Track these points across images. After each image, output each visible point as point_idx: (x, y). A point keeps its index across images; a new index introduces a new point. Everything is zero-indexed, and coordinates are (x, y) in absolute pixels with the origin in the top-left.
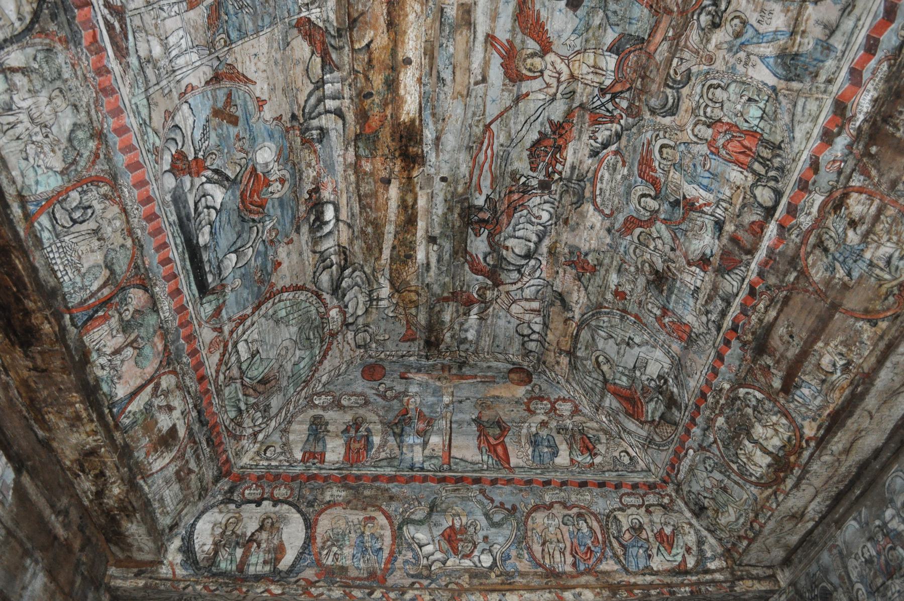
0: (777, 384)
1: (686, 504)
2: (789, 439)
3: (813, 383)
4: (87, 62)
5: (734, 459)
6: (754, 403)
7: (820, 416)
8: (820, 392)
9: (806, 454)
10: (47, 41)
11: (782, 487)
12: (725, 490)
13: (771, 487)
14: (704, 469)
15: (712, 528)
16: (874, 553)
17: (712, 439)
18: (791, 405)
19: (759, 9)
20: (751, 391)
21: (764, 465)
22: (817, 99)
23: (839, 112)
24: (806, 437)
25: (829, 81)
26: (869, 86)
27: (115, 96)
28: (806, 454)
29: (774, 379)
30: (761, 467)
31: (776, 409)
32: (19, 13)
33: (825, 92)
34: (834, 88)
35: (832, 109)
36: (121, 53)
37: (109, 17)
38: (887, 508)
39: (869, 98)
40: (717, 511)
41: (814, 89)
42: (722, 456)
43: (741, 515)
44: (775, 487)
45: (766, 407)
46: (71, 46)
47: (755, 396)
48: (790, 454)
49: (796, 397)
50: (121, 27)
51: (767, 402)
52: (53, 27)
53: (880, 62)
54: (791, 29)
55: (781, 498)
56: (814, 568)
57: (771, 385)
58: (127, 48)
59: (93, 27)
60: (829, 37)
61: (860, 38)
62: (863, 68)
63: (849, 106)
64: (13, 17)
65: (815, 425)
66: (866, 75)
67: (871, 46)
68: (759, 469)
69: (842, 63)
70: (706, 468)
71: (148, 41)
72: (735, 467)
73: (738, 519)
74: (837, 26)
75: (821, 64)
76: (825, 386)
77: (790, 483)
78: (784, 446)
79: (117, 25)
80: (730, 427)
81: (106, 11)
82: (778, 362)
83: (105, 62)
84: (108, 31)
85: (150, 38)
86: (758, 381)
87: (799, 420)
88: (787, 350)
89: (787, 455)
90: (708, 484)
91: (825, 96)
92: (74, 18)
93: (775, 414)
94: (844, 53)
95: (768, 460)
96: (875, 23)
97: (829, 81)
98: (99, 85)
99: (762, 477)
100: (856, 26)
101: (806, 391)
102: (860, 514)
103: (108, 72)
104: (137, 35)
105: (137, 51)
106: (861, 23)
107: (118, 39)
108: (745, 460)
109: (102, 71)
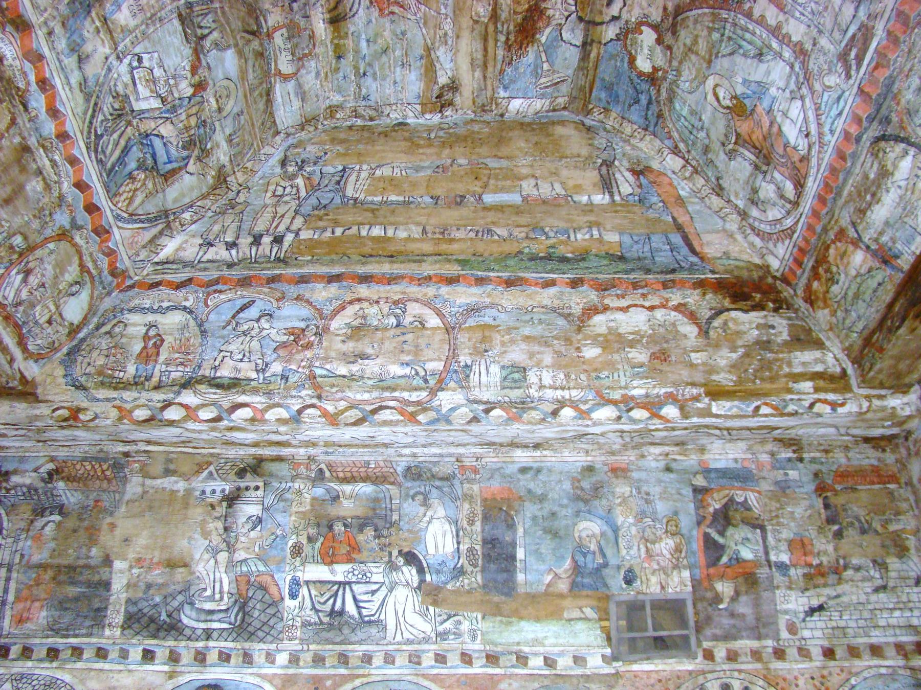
4: (897, 58)
10: (905, 118)
19: (146, 8)
22: (46, 10)
23: (18, 21)
25: (50, 33)
26: (18, 63)
27: (901, 8)
32: (903, 156)
33: (46, 23)
34: (41, 33)
35: (26, 17)
36: (866, 32)
37: (854, 67)
39: (8, 56)
41: (55, 13)
46: (895, 89)
50: (850, 50)
52: (895, 118)
53: (28, 84)
54: (109, 22)
58: (859, 29)
59: (871, 74)
60: (79, 56)
61: (58, 82)
62: (36, 68)
63: (15, 34)
64: (909, 158)
66: (28, 66)
67: (44, 84)
69: (54, 55)
71: (840, 9)
74: (80, 68)
75: (68, 35)
79: (853, 54)
81: (853, 73)
83: (884, 42)
84: (863, 60)
85: (837, 9)
91: (42, 19)
92: (879, 95)
94: (60, 61)
96: (58, 98)
97: (50, 33)
98: (905, 32)
100: (69, 83)
103: (889, 33)
104: (845, 28)
105: (854, 16)
106: (67, 89)
107: (860, 45)
109: (893, 39)
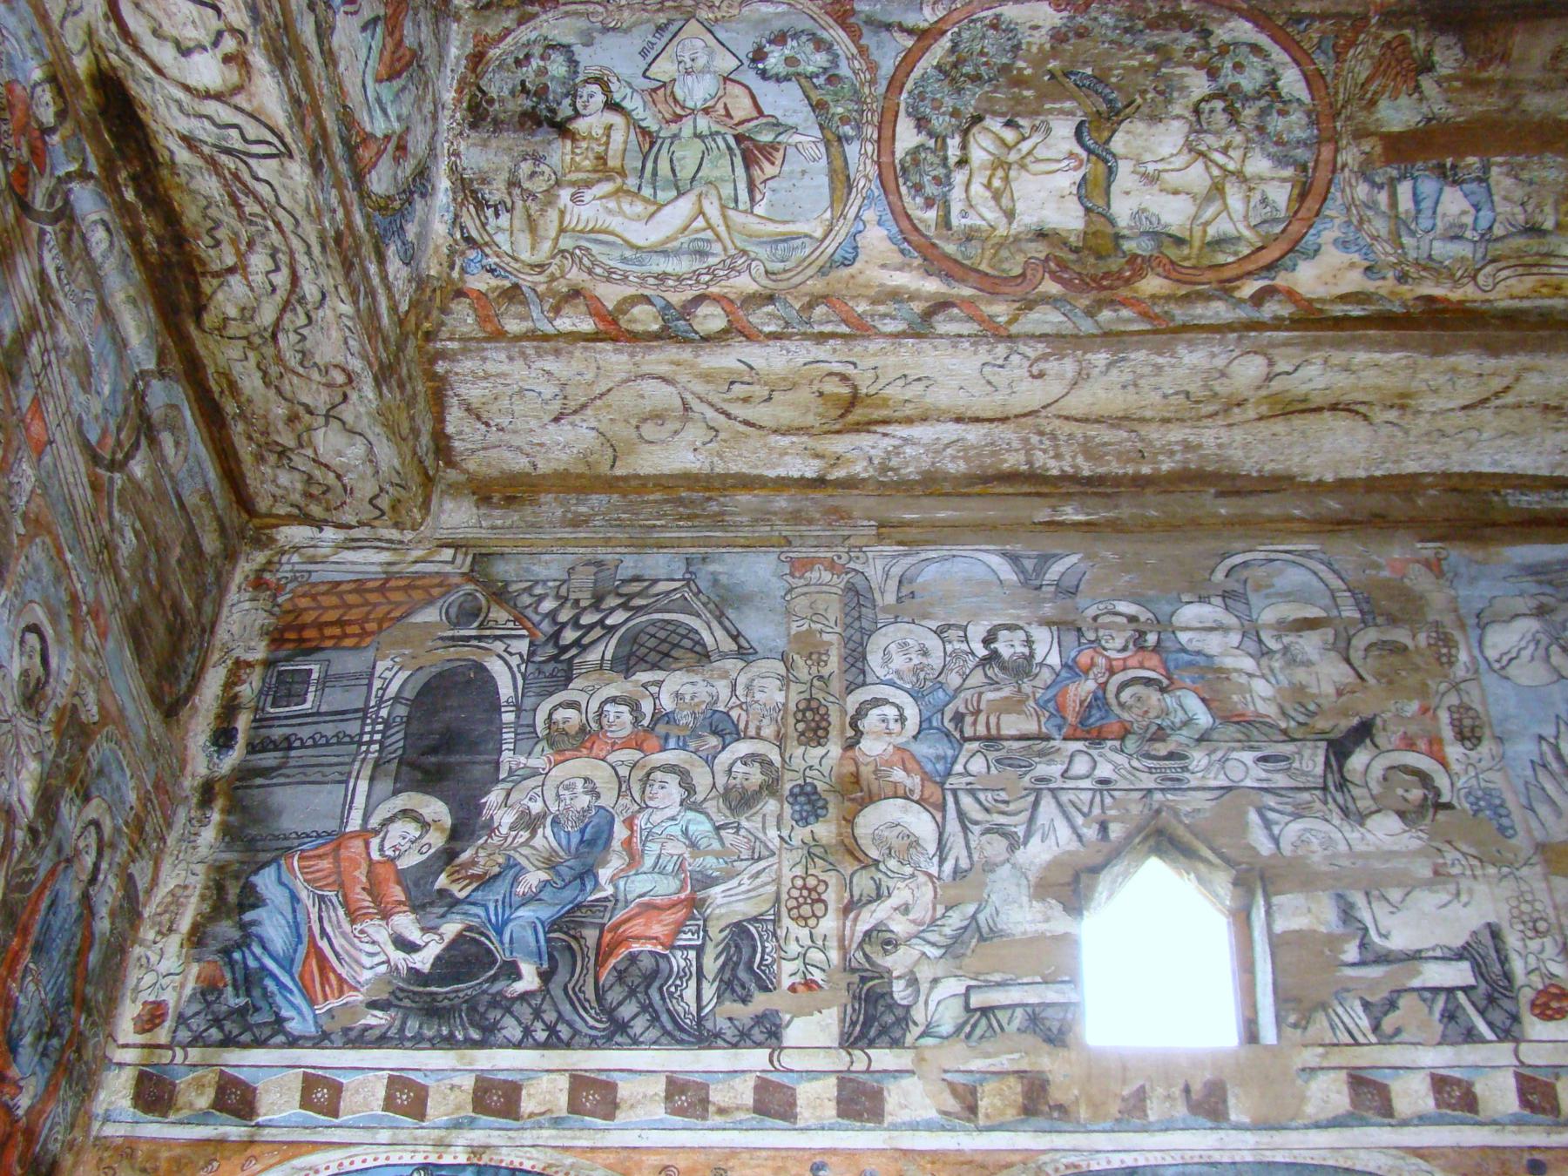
0: (1397, 114)
1: (477, 59)
2: (1220, 243)
3: (1503, 208)
5: (939, 123)
6: (1251, 80)
7: (1403, 278)
8: (1487, 237)
9: (1219, 311)
11: (1000, 311)
12: (751, 152)
13: (948, 276)
14: (745, 48)
15: (496, 192)
16: (1054, 660)
17: (911, 20)
18: (1362, 191)
20: (1278, 55)
21: (1029, 216)
24: (1282, 280)
28: (1219, 311)
29: (1403, 100)
30: (1010, 215)
31: (1301, 154)
38: (1203, 599)
40: (602, 168)
42: (895, 84)
43: (702, 254)
44: (967, 291)
45: (1276, 123)
47: (1273, 76)
48: (1172, 270)
49: (1404, 189)
51: (1297, 117)
55: (943, 326)
56: (661, 565)
57: (1373, 103)
65: (1354, 281)
68: (991, 214)
70: (759, 55)
72: (907, 137)
73: (661, 251)
76: (1520, 241)
77: (1046, 319)
78: (1179, 242)
80: (1055, 53)
82: (1473, 84)
86: (1339, 57)
87: (1328, 233)
88: (1541, 87)
89: (1138, 266)
90: (697, 91)
93: (1281, 161)
95: (1069, 219)
99: (969, 236)
101: (1454, 203)
102: (1046, 560)
108: (978, 155)
